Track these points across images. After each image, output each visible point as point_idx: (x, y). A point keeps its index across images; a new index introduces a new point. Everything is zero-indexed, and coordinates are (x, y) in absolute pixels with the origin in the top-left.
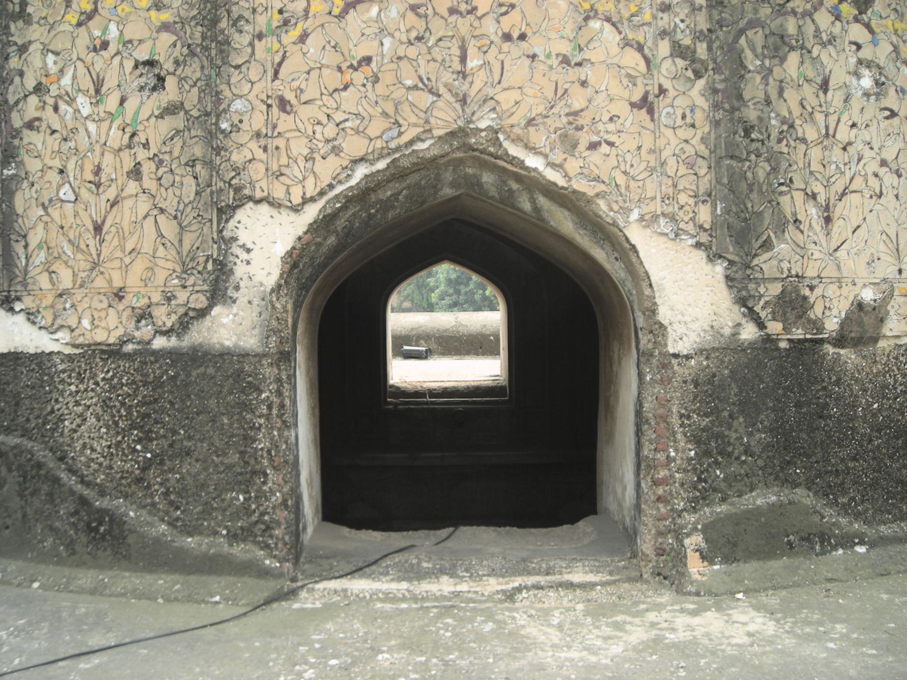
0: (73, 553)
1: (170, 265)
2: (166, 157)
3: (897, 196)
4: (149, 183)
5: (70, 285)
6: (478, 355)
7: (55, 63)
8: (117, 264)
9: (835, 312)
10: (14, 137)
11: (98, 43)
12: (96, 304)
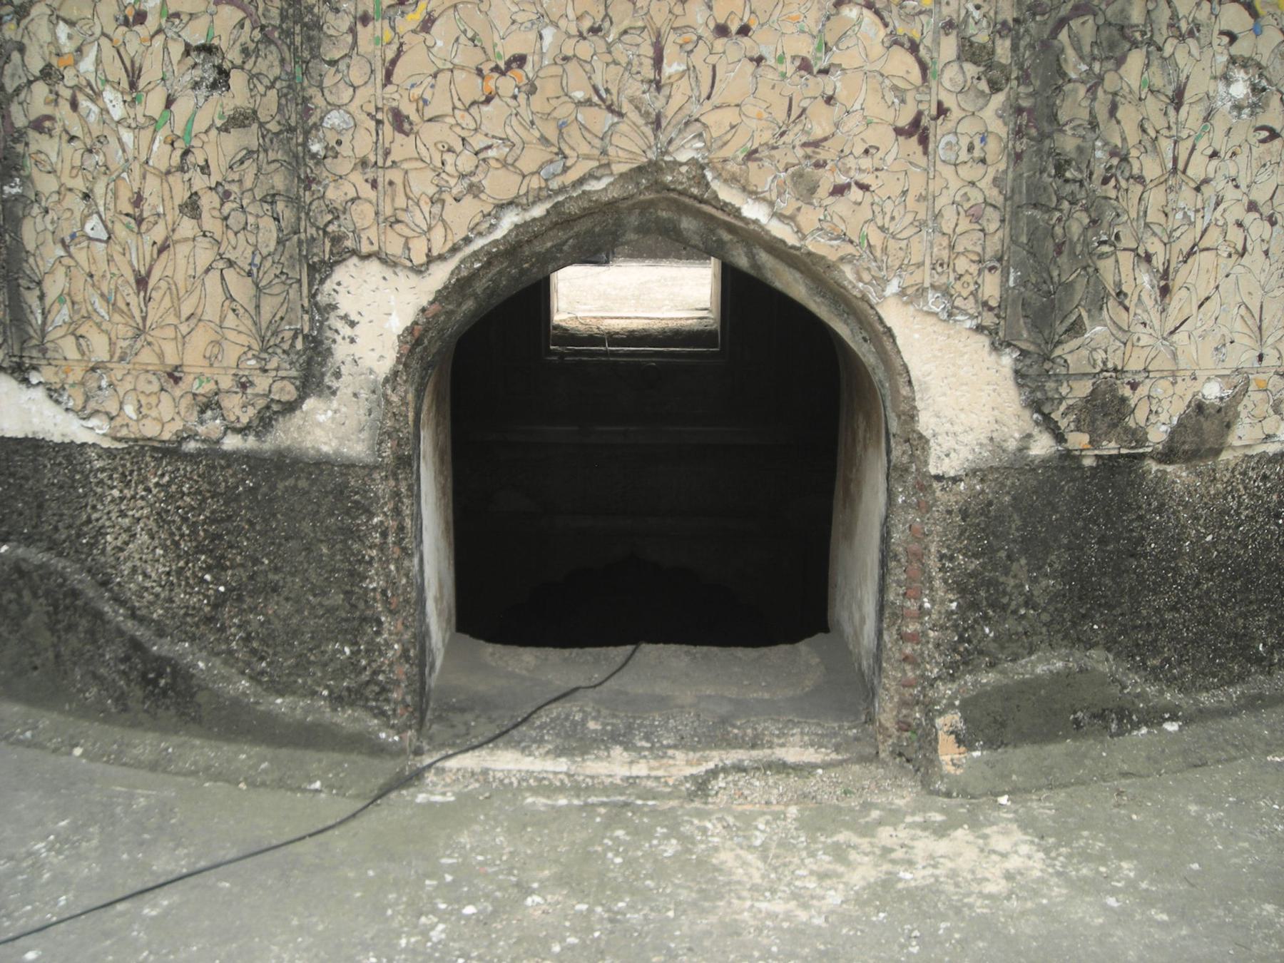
0: (125, 709)
1: (244, 340)
2: (234, 188)
3: (1266, 253)
4: (211, 223)
5: (106, 357)
6: (680, 259)
7: (70, 37)
8: (170, 332)
9: (1164, 417)
10: (16, 140)
11: (130, 13)
12: (142, 385)
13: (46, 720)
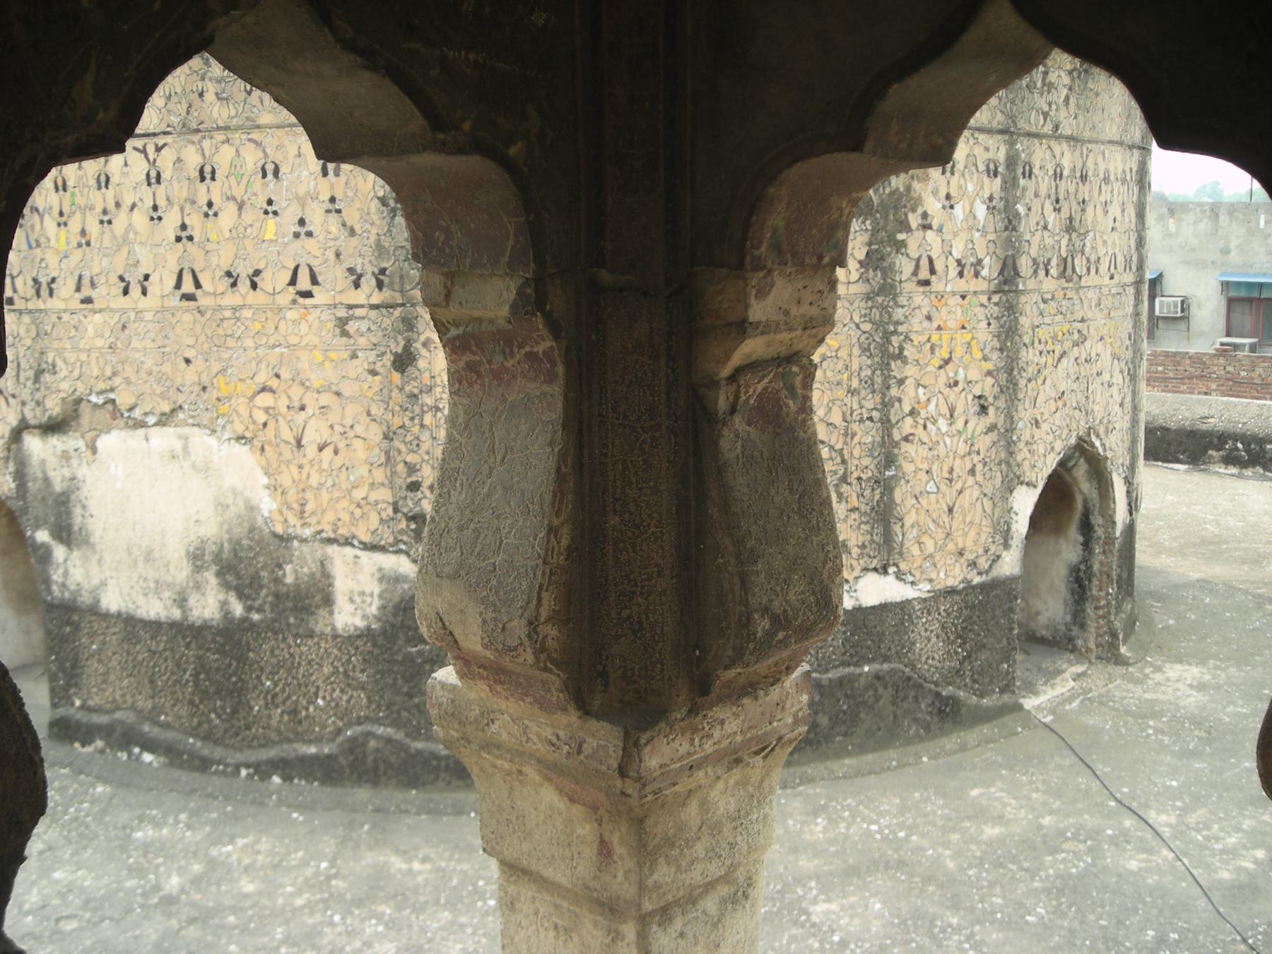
1: (987, 530)
11: (952, 381)
12: (949, 562)
13: (892, 753)
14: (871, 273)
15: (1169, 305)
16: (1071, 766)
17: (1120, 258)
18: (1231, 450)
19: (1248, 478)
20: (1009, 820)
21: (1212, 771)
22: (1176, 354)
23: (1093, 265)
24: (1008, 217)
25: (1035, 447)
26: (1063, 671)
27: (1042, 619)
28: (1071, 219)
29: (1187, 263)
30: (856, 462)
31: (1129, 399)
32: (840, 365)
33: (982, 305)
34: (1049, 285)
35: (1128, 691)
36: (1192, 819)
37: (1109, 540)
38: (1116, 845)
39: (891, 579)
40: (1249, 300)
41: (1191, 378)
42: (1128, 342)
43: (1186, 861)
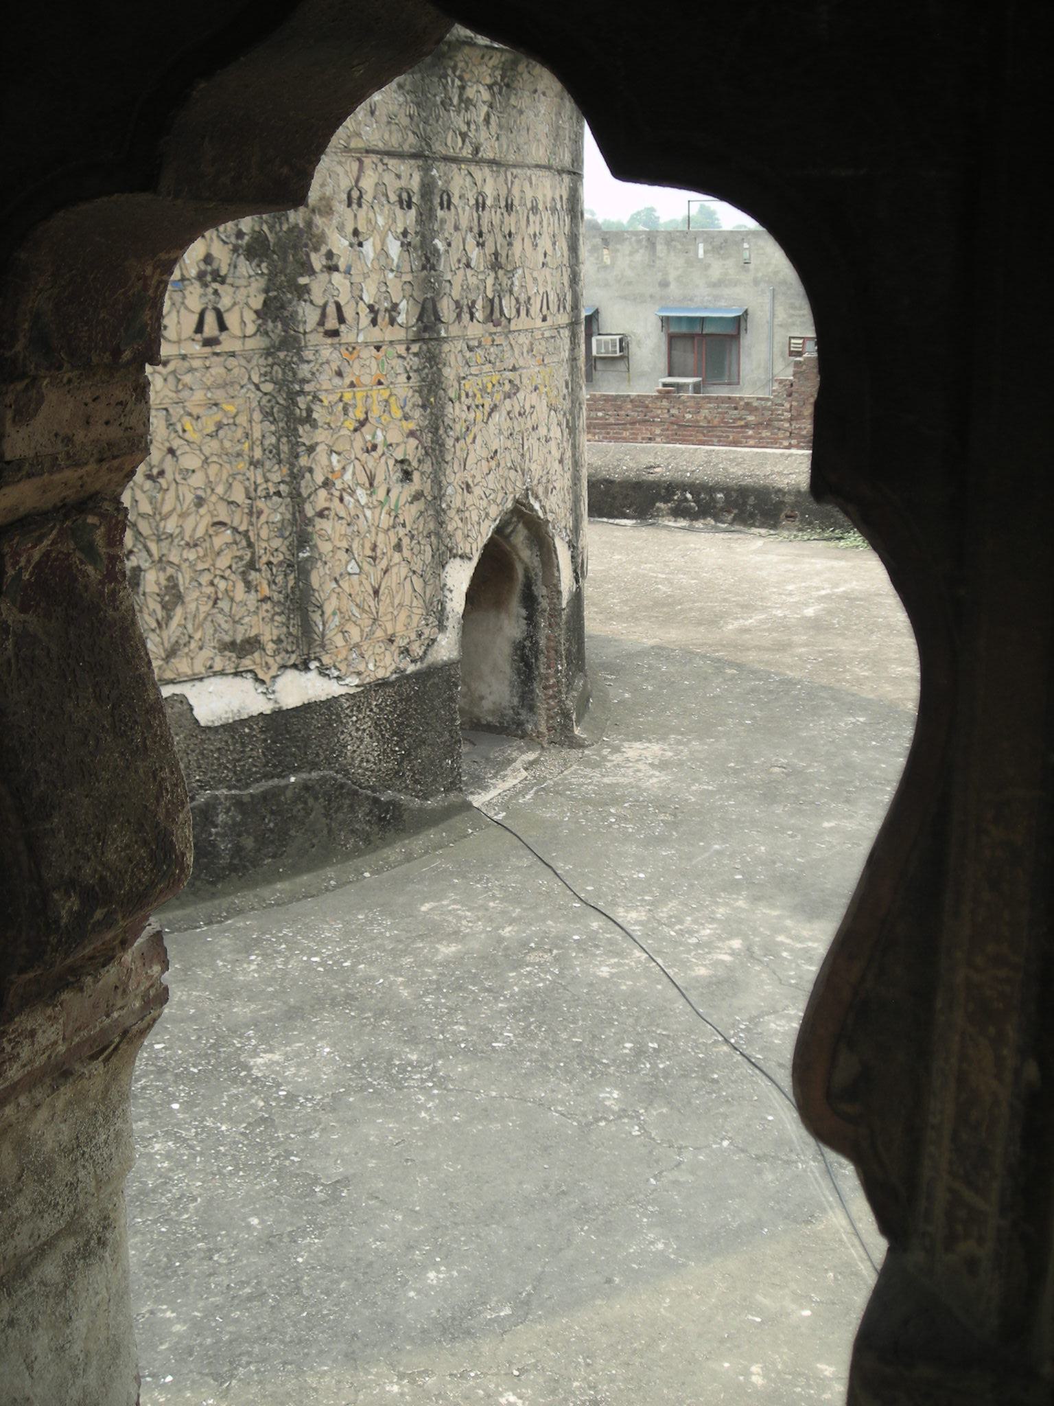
0: (370, 842)
1: (420, 611)
2: (415, 532)
4: (406, 553)
7: (339, 461)
8: (389, 617)
10: (307, 525)
12: (378, 650)
13: (330, 872)
14: (270, 325)
15: (606, 343)
16: (529, 867)
17: (552, 297)
18: (680, 501)
19: (698, 530)
20: (465, 936)
21: (680, 858)
22: (616, 398)
23: (523, 306)
24: (424, 253)
25: (467, 514)
26: (514, 760)
27: (487, 704)
28: (496, 254)
29: (625, 298)
30: (264, 545)
31: (568, 454)
32: (239, 433)
33: (400, 356)
34: (475, 330)
35: (585, 776)
36: (663, 913)
37: (555, 612)
38: (585, 950)
39: (313, 675)
40: (691, 337)
41: (633, 423)
42: (565, 391)
43: (660, 961)
